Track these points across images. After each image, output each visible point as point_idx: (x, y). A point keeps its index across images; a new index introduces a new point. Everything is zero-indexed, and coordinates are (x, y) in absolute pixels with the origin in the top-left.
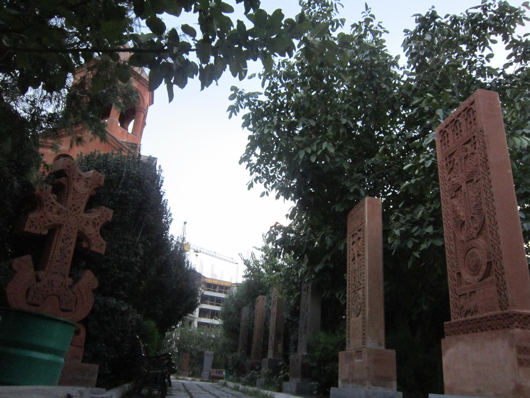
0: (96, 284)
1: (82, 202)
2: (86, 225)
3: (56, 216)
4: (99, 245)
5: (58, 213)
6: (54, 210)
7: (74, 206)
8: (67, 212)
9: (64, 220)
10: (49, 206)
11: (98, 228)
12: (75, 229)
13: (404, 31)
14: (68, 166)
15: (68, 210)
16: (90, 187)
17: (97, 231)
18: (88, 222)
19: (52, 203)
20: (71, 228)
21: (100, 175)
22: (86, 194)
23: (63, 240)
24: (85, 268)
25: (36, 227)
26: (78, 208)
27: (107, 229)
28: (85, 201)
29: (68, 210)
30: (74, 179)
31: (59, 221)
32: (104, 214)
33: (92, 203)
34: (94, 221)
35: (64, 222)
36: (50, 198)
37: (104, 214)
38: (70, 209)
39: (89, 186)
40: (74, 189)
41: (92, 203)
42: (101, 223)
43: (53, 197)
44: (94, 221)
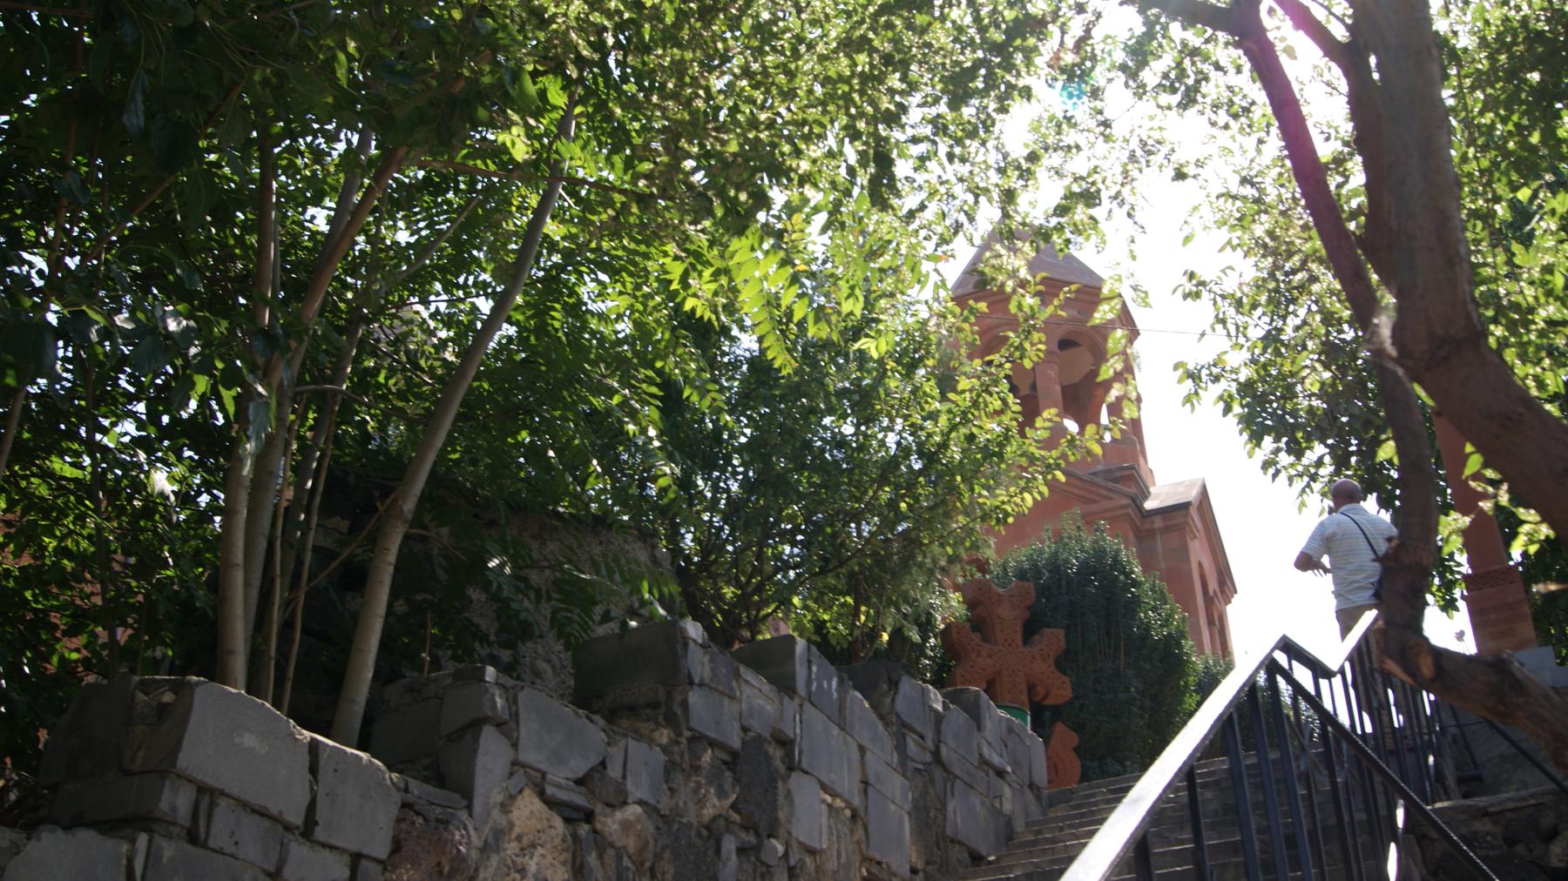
0: (1074, 739)
4: (1060, 690)
5: (990, 656)
6: (984, 653)
11: (1051, 661)
13: (1176, 367)
21: (1026, 584)
24: (1053, 722)
27: (1064, 662)
28: (1019, 628)
32: (1053, 638)
33: (1030, 629)
37: (1053, 638)
41: (1030, 629)
43: (976, 637)
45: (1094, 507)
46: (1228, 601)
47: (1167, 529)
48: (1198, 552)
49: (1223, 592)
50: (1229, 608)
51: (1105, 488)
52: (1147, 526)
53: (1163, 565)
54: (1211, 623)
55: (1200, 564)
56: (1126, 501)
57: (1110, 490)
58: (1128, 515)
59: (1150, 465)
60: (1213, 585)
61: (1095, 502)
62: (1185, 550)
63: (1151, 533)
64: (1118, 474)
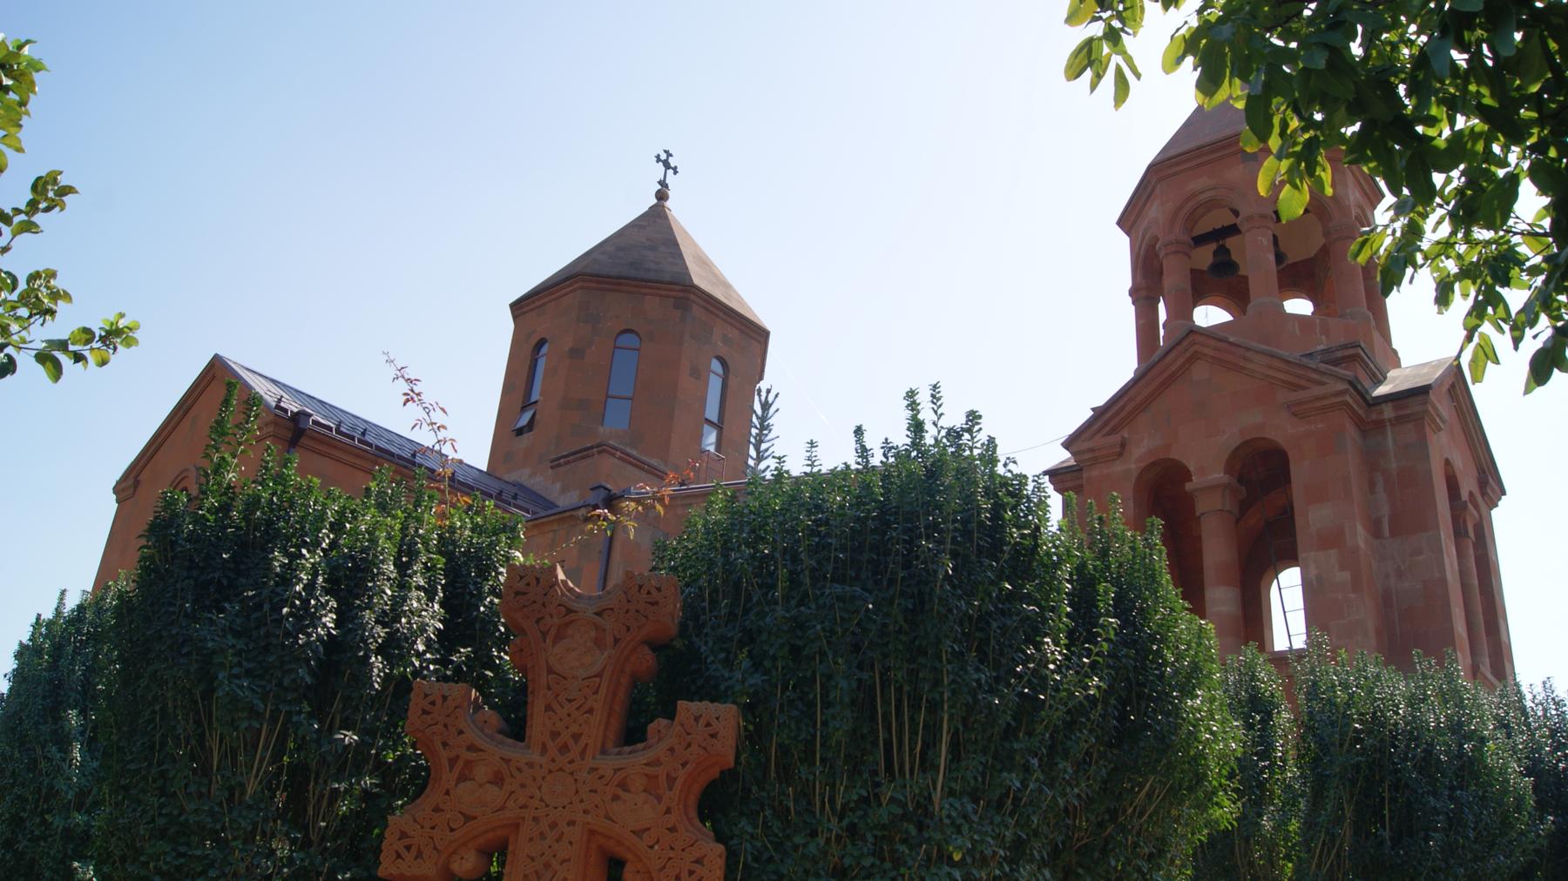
1: (590, 711)
2: (616, 798)
3: (494, 794)
5: (498, 780)
6: (481, 772)
7: (555, 735)
8: (530, 765)
9: (522, 801)
10: (460, 763)
12: (571, 823)
14: (517, 593)
15: (536, 757)
16: (616, 641)
17: (668, 811)
18: (623, 785)
19: (472, 748)
20: (553, 825)
22: (599, 675)
23: (525, 876)
25: (419, 855)
26: (576, 737)
29: (536, 757)
30: (544, 634)
31: (502, 808)
34: (650, 770)
35: (524, 807)
36: (461, 732)
38: (544, 749)
39: (609, 640)
40: (550, 671)
42: (682, 774)
44: (650, 770)
45: (1301, 395)
46: (1493, 504)
47: (1399, 420)
48: (1443, 447)
49: (1483, 494)
50: (1494, 512)
51: (1316, 371)
52: (1374, 416)
53: (1394, 466)
54: (1459, 533)
55: (1447, 462)
56: (1342, 386)
57: (1322, 373)
58: (1346, 404)
59: (1395, 345)
60: (1468, 486)
61: (1304, 388)
62: (1423, 443)
63: (1380, 425)
64: (1339, 354)
